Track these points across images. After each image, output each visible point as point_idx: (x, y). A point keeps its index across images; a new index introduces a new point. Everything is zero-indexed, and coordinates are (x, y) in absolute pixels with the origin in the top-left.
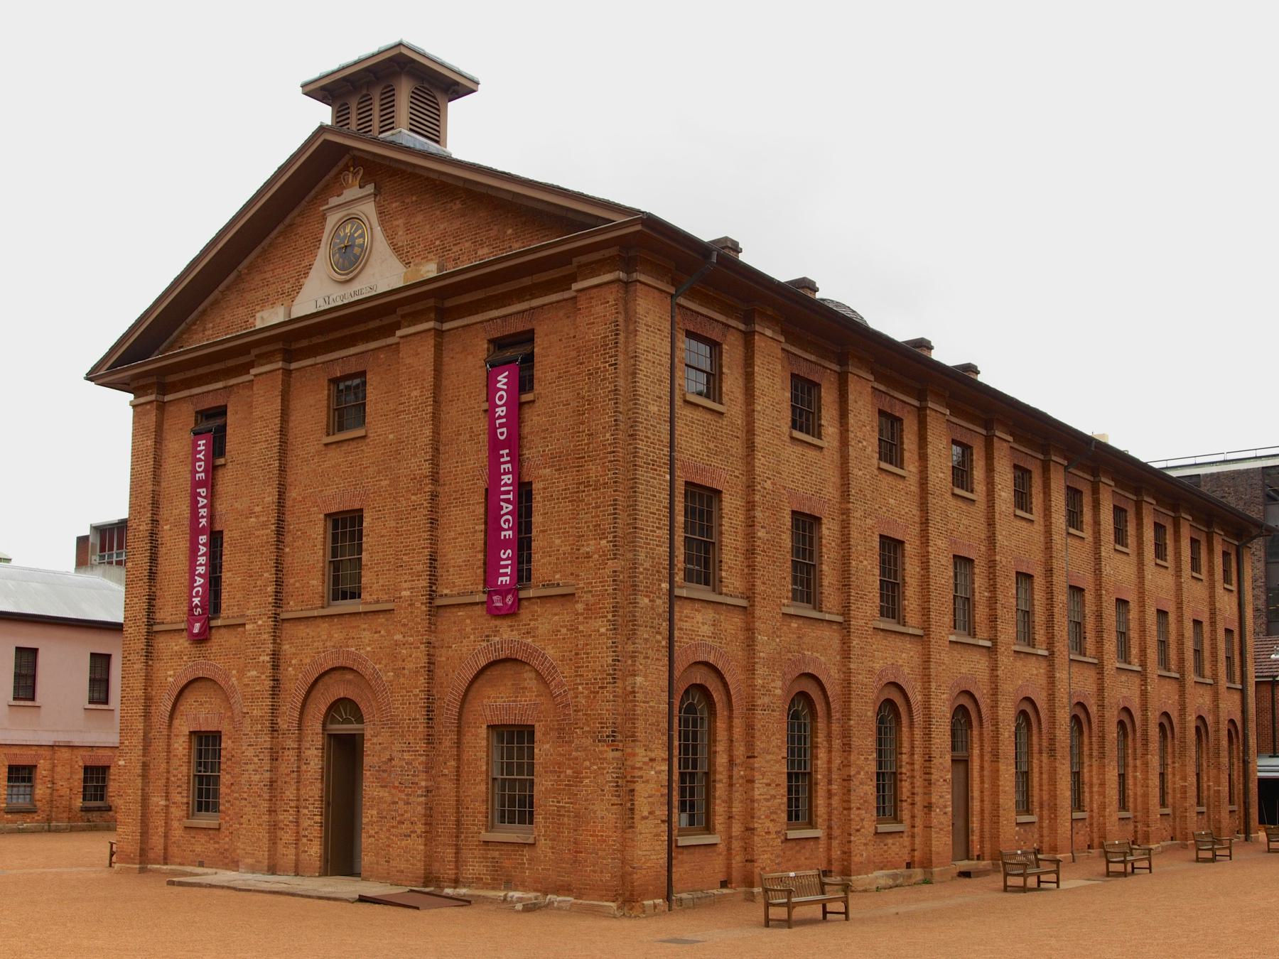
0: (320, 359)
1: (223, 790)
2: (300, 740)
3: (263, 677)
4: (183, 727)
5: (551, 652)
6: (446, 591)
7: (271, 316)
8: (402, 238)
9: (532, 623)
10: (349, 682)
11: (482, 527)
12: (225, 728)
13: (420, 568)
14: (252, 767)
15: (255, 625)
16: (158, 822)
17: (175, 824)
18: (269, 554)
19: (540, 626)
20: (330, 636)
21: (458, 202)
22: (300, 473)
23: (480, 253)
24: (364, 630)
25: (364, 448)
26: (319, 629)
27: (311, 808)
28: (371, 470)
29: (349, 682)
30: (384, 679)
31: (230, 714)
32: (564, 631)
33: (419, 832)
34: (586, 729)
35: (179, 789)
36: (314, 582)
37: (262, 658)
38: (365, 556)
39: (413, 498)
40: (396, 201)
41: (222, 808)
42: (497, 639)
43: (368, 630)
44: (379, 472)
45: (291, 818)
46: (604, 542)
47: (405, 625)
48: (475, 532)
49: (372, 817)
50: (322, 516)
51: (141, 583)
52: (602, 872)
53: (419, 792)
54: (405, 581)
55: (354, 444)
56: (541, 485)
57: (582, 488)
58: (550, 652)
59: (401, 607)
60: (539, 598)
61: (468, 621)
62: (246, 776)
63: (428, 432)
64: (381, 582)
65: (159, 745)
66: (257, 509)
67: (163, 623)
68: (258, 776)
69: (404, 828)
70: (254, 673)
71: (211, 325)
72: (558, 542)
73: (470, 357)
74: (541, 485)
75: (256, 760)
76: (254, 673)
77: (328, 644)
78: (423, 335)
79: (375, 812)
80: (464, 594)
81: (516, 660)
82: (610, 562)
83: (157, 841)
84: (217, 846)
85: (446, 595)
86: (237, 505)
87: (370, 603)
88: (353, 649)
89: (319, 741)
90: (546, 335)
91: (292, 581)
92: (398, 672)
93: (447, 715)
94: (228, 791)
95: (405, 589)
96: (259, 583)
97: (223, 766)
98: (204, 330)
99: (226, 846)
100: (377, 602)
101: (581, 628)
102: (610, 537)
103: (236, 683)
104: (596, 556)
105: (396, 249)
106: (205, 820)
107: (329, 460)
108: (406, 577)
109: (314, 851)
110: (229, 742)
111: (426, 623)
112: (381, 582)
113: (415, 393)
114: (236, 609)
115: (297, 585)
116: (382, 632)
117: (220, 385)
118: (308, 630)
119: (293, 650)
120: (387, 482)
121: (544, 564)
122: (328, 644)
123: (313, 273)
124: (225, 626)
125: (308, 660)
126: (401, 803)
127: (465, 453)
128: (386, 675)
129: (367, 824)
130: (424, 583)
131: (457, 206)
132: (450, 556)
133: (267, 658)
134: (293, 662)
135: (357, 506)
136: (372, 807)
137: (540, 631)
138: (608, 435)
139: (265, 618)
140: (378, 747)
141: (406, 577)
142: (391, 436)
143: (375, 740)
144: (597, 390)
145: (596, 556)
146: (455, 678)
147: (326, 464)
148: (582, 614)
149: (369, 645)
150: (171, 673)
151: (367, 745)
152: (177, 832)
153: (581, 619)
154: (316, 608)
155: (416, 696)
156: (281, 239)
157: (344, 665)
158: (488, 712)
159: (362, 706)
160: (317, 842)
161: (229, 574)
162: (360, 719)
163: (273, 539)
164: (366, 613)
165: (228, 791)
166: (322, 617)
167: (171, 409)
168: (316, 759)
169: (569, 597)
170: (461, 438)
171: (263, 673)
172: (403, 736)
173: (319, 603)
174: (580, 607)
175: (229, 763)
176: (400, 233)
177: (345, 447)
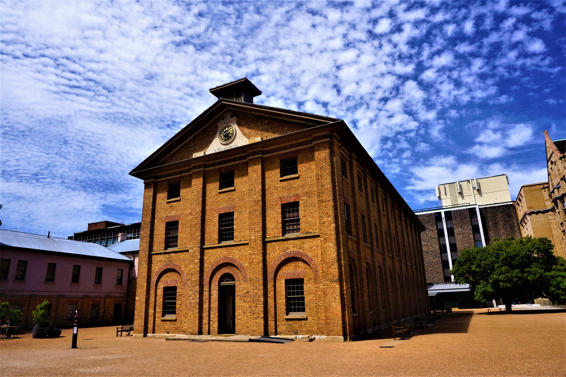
1: (177, 306)
3: (196, 267)
4: (161, 286)
5: (310, 254)
7: (200, 154)
11: (281, 216)
12: (178, 285)
14: (192, 297)
16: (151, 319)
17: (157, 319)
18: (199, 227)
27: (214, 311)
28: (237, 200)
30: (244, 266)
31: (180, 280)
32: (314, 247)
33: (261, 317)
34: (327, 278)
35: (159, 307)
36: (215, 236)
37: (195, 261)
38: (235, 227)
41: (177, 312)
42: (288, 251)
46: (330, 218)
47: (253, 248)
50: (218, 215)
51: (146, 238)
52: (337, 326)
53: (261, 303)
56: (303, 202)
57: (320, 202)
58: (310, 254)
59: (251, 242)
61: (276, 246)
62: (189, 301)
63: (260, 187)
65: (152, 292)
66: (193, 213)
68: (194, 301)
69: (255, 316)
70: (193, 266)
72: (310, 219)
73: (273, 165)
74: (303, 202)
75: (193, 295)
76: (193, 266)
77: (221, 255)
79: (240, 311)
80: (274, 237)
83: (150, 325)
84: (175, 326)
89: (217, 288)
92: (251, 263)
93: (270, 276)
94: (179, 307)
96: (194, 236)
97: (177, 298)
98: (172, 159)
99: (179, 326)
100: (240, 241)
101: (323, 246)
102: (332, 217)
103: (184, 270)
105: (244, 134)
106: (168, 317)
108: (253, 232)
109: (215, 326)
110: (180, 290)
113: (254, 176)
114: (184, 246)
115: (208, 237)
122: (221, 255)
125: (213, 261)
126: (253, 307)
127: (273, 193)
129: (237, 315)
130: (260, 233)
133: (198, 261)
134: (207, 262)
135: (231, 211)
136: (239, 309)
137: (305, 247)
138: (329, 186)
139: (197, 248)
140: (241, 289)
141: (253, 232)
142: (244, 189)
143: (240, 286)
145: (327, 223)
146: (272, 265)
151: (236, 288)
152: (158, 321)
153: (323, 243)
155: (258, 271)
158: (285, 275)
159: (234, 275)
160: (217, 323)
161: (180, 234)
162: (234, 280)
165: (179, 307)
169: (318, 236)
172: (253, 284)
173: (217, 242)
175: (180, 297)
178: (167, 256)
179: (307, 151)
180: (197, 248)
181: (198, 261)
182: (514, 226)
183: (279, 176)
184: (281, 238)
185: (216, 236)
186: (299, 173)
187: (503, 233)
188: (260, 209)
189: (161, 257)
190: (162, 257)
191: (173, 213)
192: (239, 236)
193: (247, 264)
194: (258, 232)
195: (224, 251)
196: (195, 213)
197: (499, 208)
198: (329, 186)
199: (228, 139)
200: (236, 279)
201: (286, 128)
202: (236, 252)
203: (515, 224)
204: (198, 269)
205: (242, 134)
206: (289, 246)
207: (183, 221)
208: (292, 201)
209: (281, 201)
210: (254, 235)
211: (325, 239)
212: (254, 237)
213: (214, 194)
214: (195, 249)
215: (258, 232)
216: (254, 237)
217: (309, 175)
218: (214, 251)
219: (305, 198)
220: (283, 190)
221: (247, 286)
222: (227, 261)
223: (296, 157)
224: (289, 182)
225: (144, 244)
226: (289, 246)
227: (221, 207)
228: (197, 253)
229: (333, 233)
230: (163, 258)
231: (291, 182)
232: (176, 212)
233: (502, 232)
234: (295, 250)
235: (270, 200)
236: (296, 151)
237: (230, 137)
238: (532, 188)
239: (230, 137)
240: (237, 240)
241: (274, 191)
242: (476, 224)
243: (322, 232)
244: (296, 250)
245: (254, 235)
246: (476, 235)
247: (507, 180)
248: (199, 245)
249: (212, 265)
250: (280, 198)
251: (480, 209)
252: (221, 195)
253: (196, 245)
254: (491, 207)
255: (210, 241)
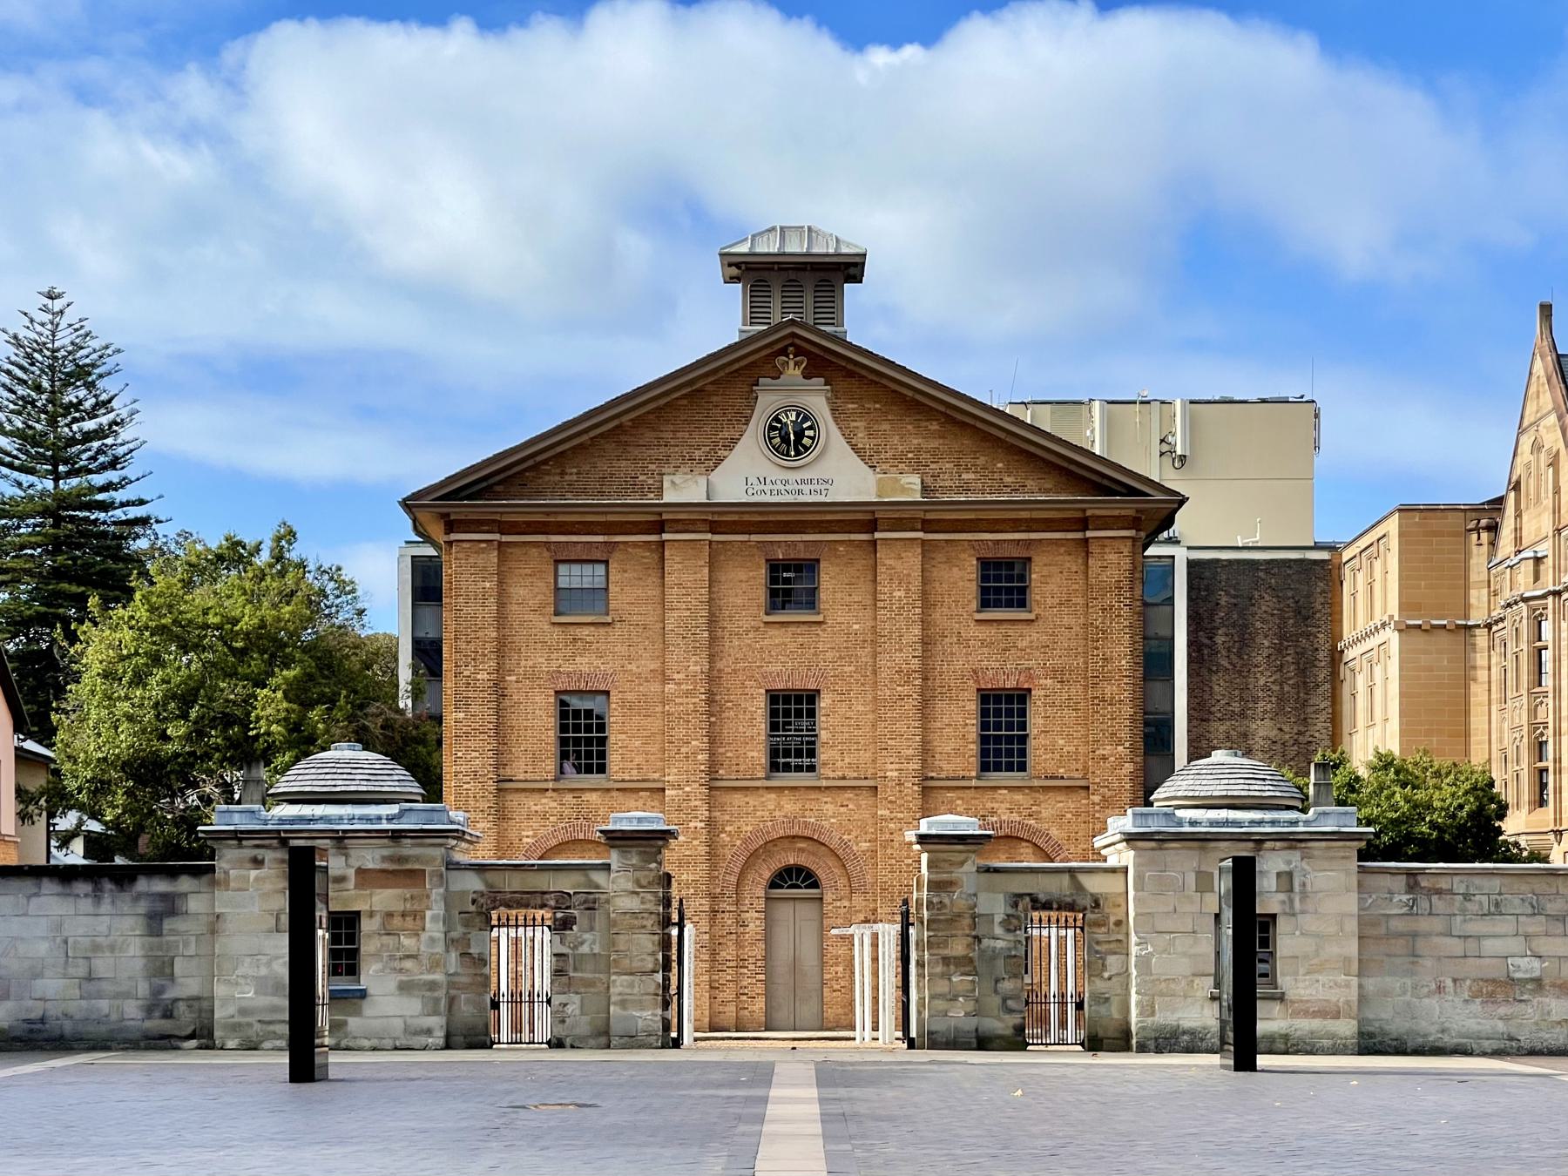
0: (754, 538)
2: (737, 903)
3: (696, 842)
5: (1056, 832)
6: (933, 774)
8: (861, 438)
9: (1034, 808)
10: (802, 850)
13: (910, 752)
15: (681, 792)
19: (1043, 811)
20: (781, 808)
21: (934, 423)
22: (733, 647)
23: (964, 476)
24: (826, 803)
25: (820, 633)
26: (764, 799)
27: (751, 967)
28: (829, 655)
29: (802, 850)
30: (854, 848)
32: (1069, 816)
36: (755, 754)
37: (692, 825)
39: (899, 688)
40: (853, 403)
42: (995, 819)
43: (832, 803)
44: (840, 658)
45: (729, 978)
47: (891, 802)
48: (967, 725)
49: (836, 973)
50: (763, 691)
54: (892, 763)
55: (805, 628)
56: (1042, 693)
57: (1096, 701)
58: (1054, 832)
60: (1041, 787)
61: (959, 802)
64: (847, 760)
66: (676, 676)
67: (511, 781)
71: (575, 470)
72: (1061, 742)
73: (955, 570)
74: (1042, 693)
77: (777, 813)
78: (907, 542)
79: (840, 969)
81: (1017, 838)
82: (1127, 765)
85: (932, 778)
86: (633, 667)
87: (834, 778)
88: (812, 820)
90: (1045, 565)
91: (721, 750)
95: (892, 770)
98: (563, 473)
100: (844, 778)
101: (1097, 815)
102: (1127, 744)
104: (1113, 759)
105: (854, 448)
107: (770, 638)
111: (919, 802)
112: (847, 760)
113: (897, 594)
114: (634, 772)
115: (729, 754)
116: (850, 806)
117: (600, 538)
118: (747, 799)
119: (727, 817)
120: (852, 668)
121: (1046, 759)
123: (738, 447)
124: (617, 790)
125: (750, 828)
127: (952, 654)
128: (857, 845)
129: (831, 979)
130: (915, 765)
131: (934, 426)
132: (935, 744)
134: (728, 829)
136: (837, 964)
137: (1044, 815)
138: (1123, 662)
142: (856, 627)
144: (1111, 623)
147: (766, 642)
148: (1099, 804)
149: (833, 817)
150: (531, 833)
153: (1097, 808)
154: (759, 779)
155: (908, 865)
156: (685, 402)
157: (800, 834)
163: (703, 707)
164: (827, 788)
166: (767, 788)
167: (509, 550)
168: (758, 922)
170: (947, 640)
171: (696, 839)
173: (761, 774)
174: (1096, 798)
176: (860, 435)
177: (792, 629)
178: (569, 797)
179: (1062, 550)
180: (697, 785)
181: (703, 825)
182: (1313, 663)
183: (974, 605)
184: (974, 783)
185: (758, 757)
186: (1037, 611)
187: (1266, 688)
188: (915, 696)
189: (544, 801)
190: (547, 803)
191: (584, 663)
192: (839, 764)
193: (865, 846)
194: (908, 759)
195: (789, 805)
196: (681, 676)
197: (1267, 572)
198: (1123, 662)
199: (798, 453)
200: (824, 883)
201: (1000, 465)
202: (830, 808)
203: (1321, 655)
204: (703, 849)
205: (849, 448)
206: (996, 805)
207: (630, 696)
208: (1011, 684)
209: (977, 682)
210: (897, 766)
211: (1104, 799)
212: (896, 774)
213: (746, 622)
214: (687, 789)
215: (908, 759)
216: (896, 774)
217: (1066, 621)
218: (752, 800)
219: (1049, 682)
220: (985, 650)
221: (864, 903)
222: (796, 831)
223: (1029, 559)
224: (1003, 629)
225: (474, 754)
226: (992, 805)
227: (775, 668)
228: (697, 803)
229: (1127, 787)
230: (555, 804)
231: (1012, 630)
232: (598, 662)
233: (1262, 682)
234: (1015, 817)
235: (941, 673)
236: (1029, 542)
237: (807, 449)
238: (1434, 522)
239: (807, 449)
240: (831, 775)
241: (955, 648)
242: (1163, 632)
243: (1097, 780)
244: (1018, 819)
245: (897, 766)
246: (1157, 687)
247: (1317, 427)
248: (705, 778)
249: (745, 841)
250: (975, 672)
251: (1192, 565)
252: (773, 632)
253: (693, 778)
254: (1238, 561)
255: (734, 768)
